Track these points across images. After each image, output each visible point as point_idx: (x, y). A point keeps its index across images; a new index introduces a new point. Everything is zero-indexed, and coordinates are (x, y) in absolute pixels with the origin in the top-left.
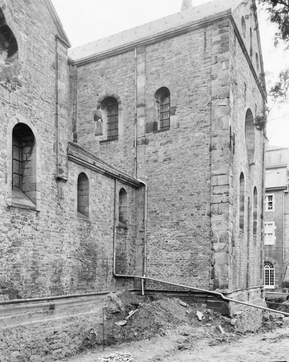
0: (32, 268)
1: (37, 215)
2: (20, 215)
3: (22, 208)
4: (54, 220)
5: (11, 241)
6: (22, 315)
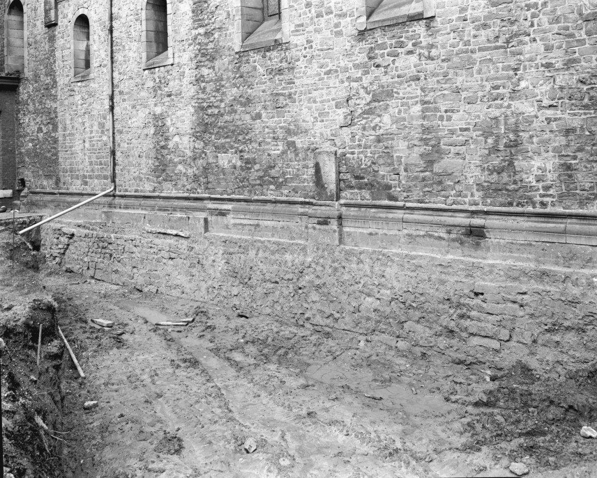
0: (421, 140)
1: (428, 27)
2: (387, 40)
3: (389, 26)
4: (482, 22)
5: (369, 94)
6: (391, 233)
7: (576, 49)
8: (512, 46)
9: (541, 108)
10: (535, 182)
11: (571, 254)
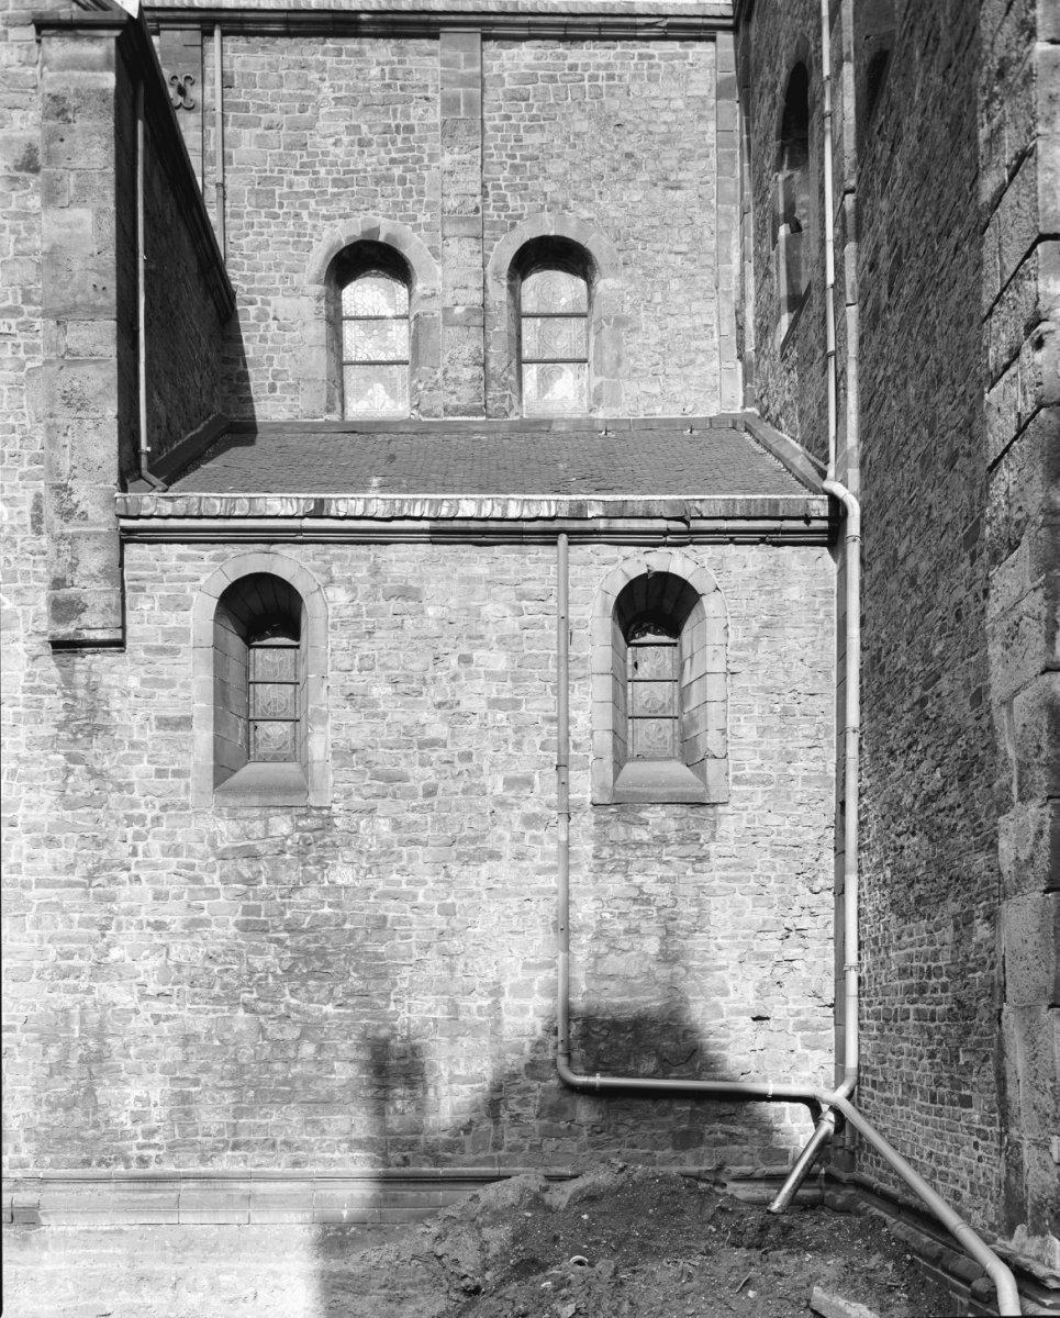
4: (46, 834)
7: (205, 903)
8: (99, 885)
9: (144, 996)
10: (130, 1123)
11: (186, 1242)
